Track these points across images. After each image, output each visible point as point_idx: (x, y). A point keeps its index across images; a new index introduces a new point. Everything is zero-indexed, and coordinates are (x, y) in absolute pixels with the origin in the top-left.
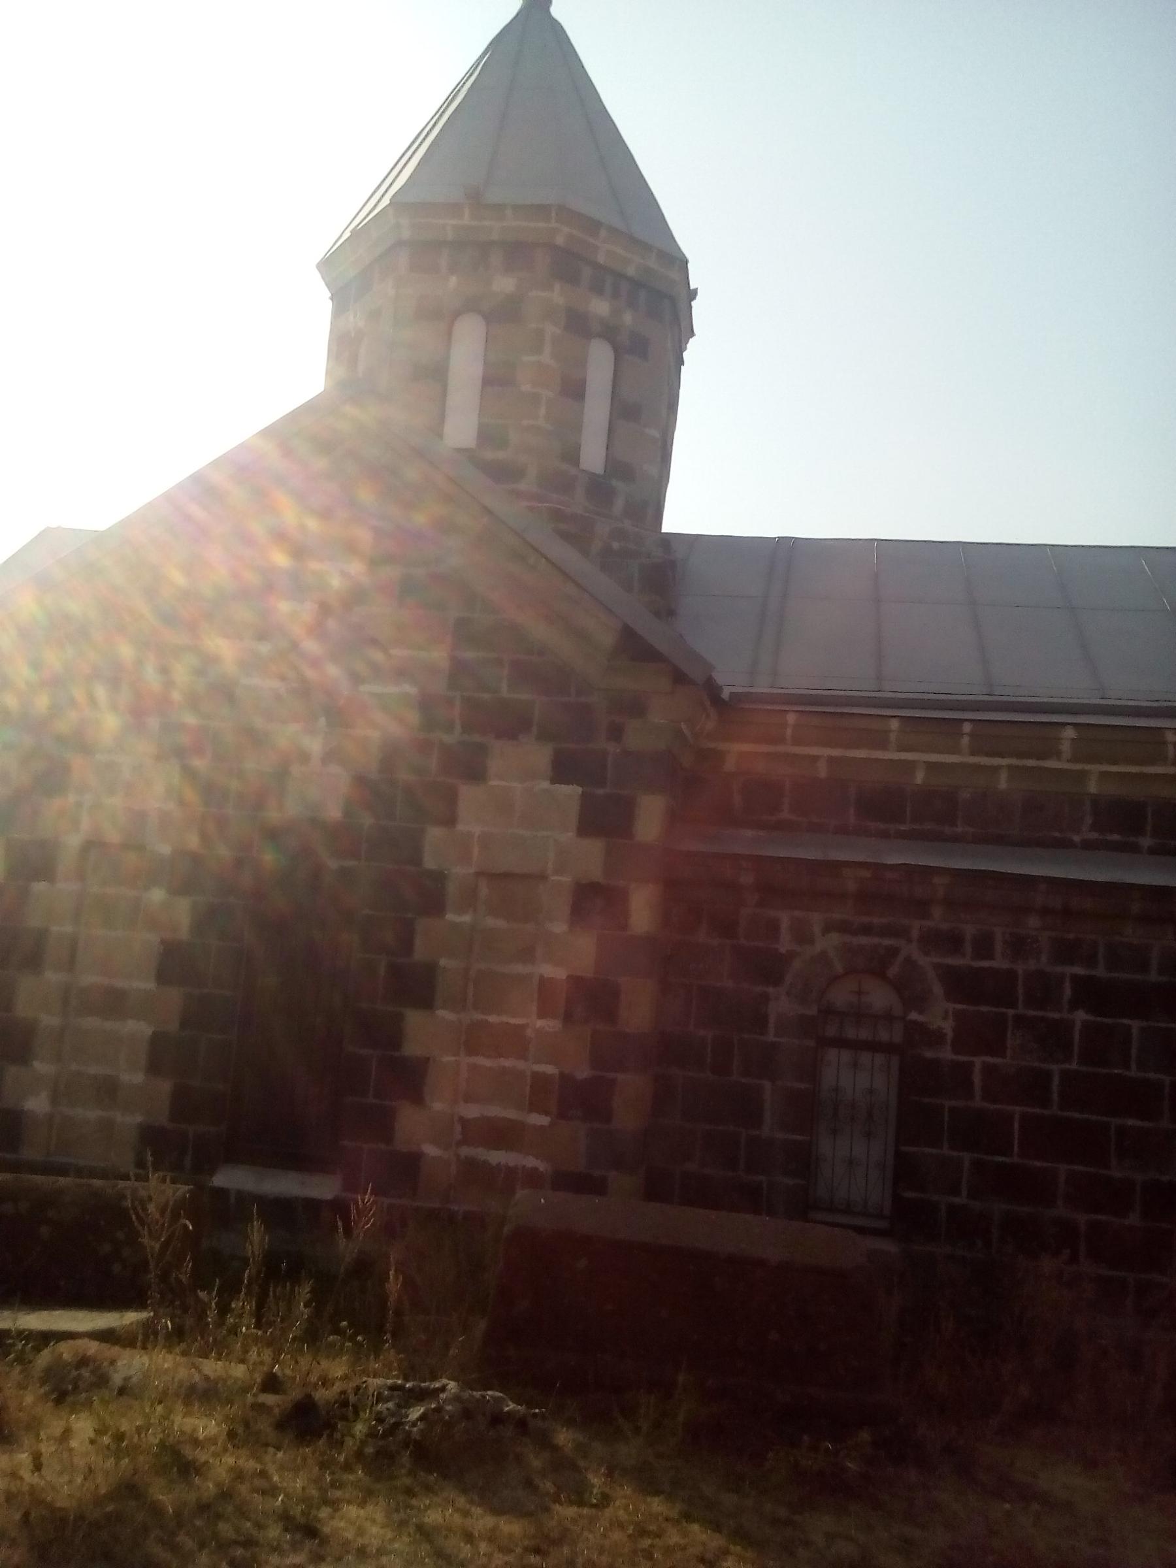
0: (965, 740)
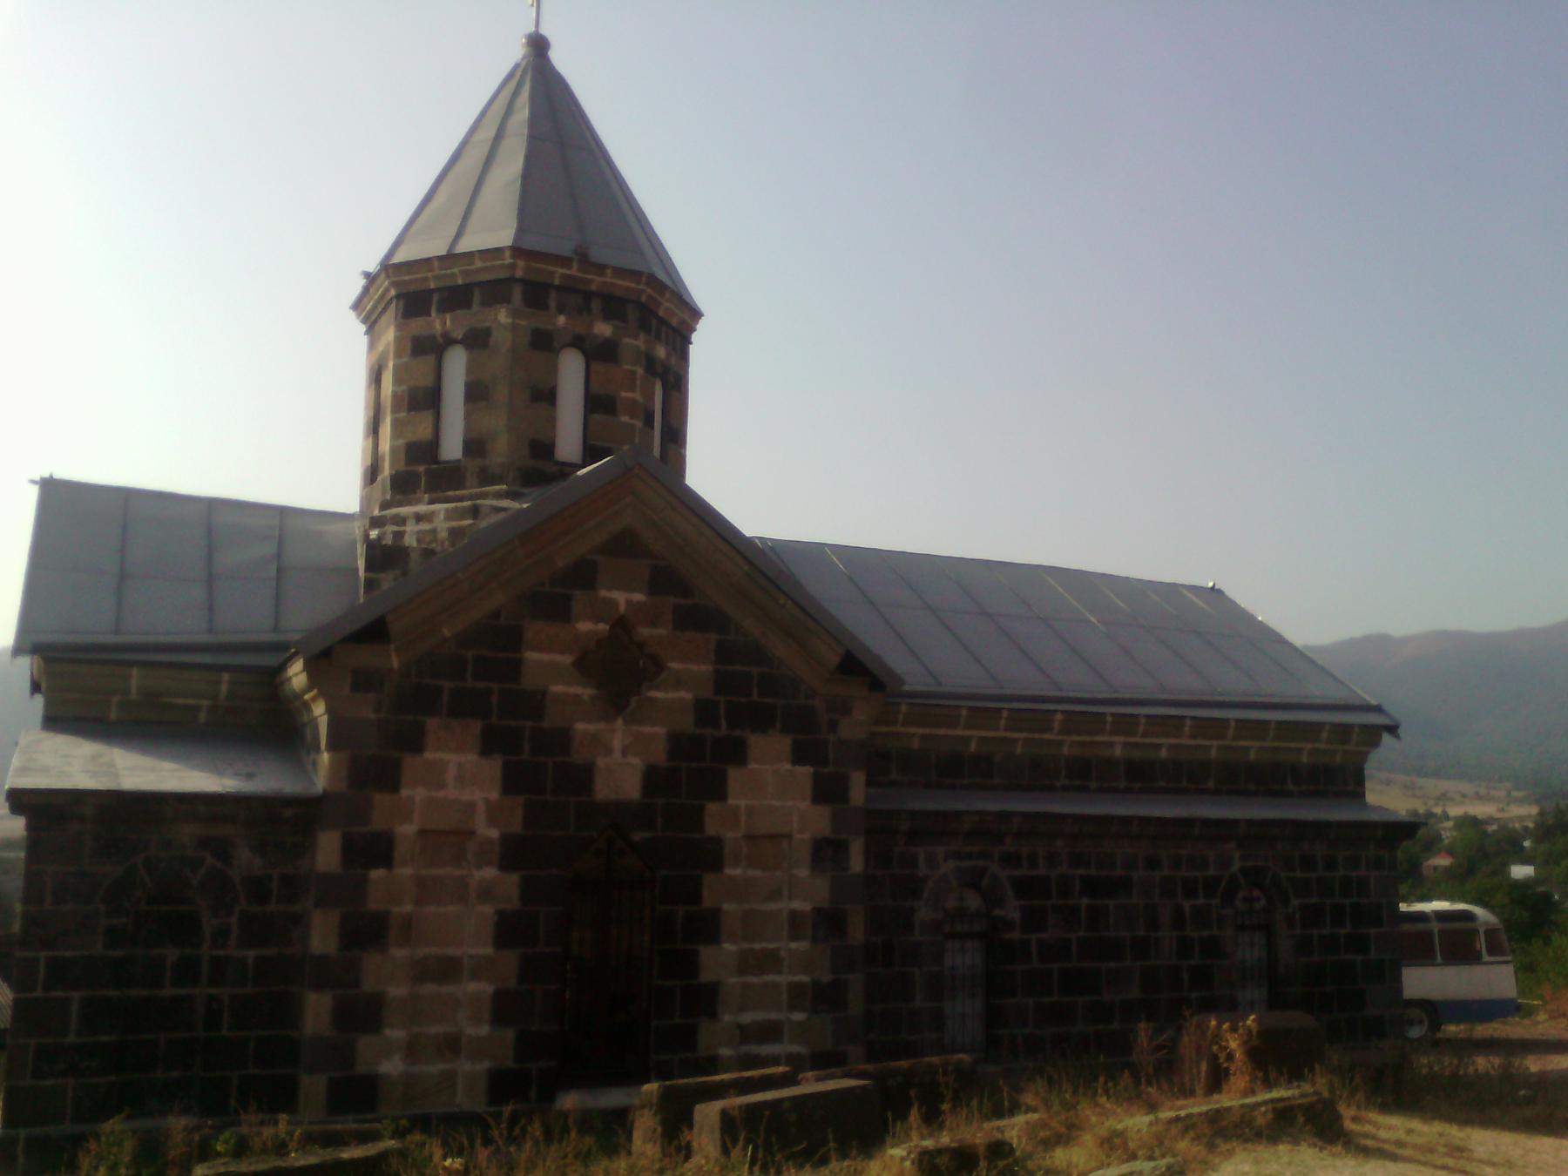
0: (1003, 722)
